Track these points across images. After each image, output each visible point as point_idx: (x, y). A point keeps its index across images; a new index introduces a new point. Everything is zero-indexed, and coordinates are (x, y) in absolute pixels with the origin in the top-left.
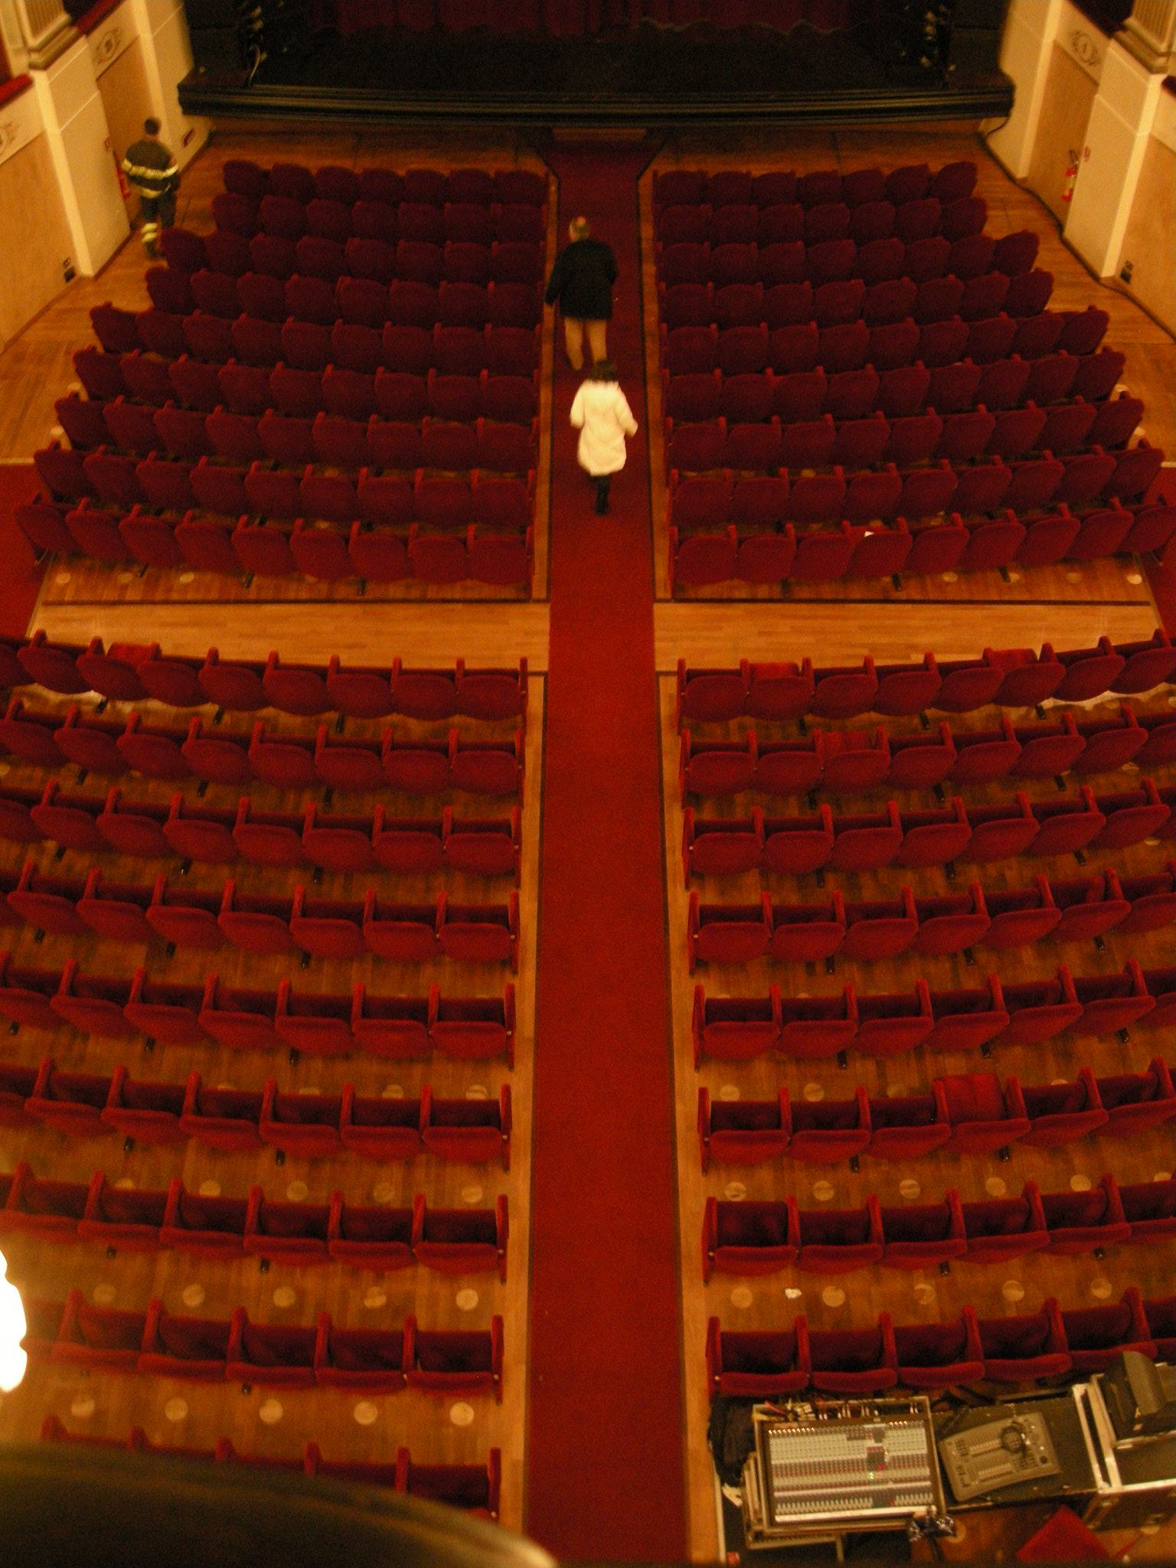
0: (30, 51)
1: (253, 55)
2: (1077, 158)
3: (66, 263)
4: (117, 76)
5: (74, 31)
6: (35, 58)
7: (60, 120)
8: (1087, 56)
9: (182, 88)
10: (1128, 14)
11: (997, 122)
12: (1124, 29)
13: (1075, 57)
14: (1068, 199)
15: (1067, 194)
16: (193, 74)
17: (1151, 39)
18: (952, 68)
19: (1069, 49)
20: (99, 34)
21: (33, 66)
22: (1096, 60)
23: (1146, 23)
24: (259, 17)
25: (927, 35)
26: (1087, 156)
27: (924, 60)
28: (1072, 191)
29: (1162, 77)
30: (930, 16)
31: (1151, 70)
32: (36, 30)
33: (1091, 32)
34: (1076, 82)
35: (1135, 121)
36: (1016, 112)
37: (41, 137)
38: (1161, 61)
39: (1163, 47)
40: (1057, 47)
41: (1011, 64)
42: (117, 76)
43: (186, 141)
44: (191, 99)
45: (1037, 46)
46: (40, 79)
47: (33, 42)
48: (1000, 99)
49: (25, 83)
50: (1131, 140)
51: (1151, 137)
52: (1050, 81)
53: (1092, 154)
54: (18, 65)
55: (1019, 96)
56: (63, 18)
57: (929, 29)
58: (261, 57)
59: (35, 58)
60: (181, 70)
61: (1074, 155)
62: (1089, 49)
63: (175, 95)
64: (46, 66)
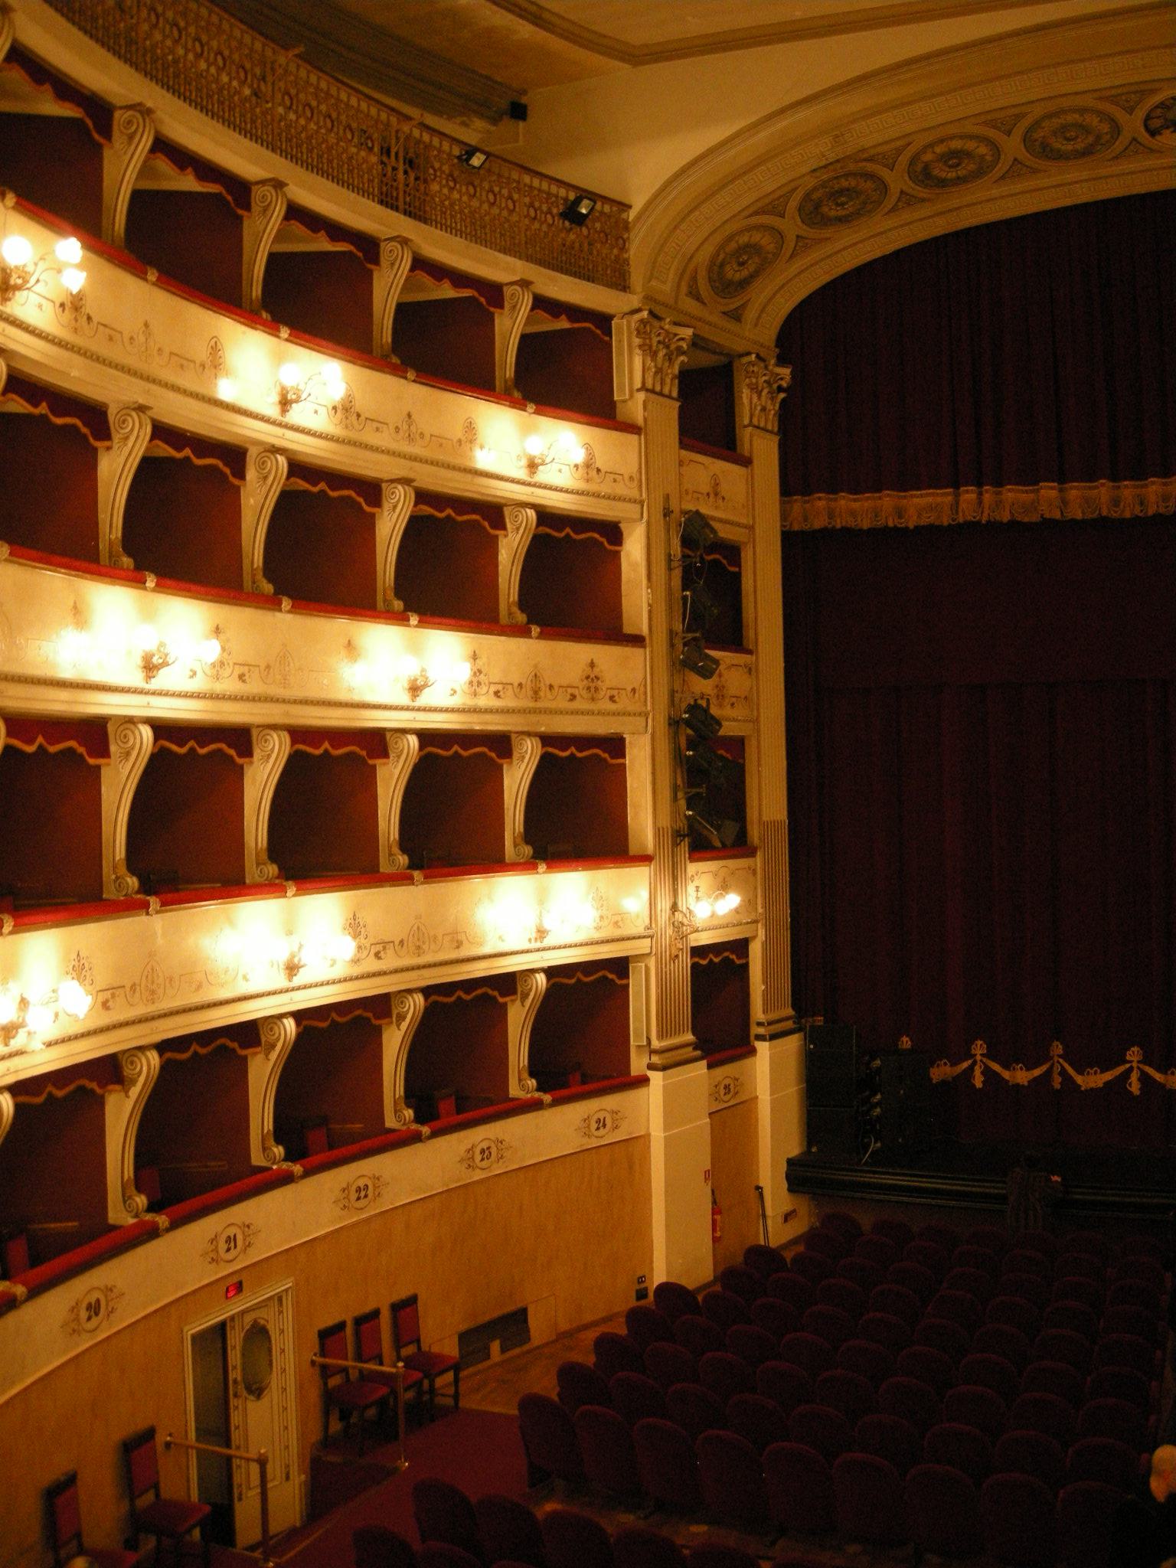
0: (653, 1052)
1: (866, 1147)
3: (641, 1280)
4: (730, 1120)
5: (698, 1053)
6: (655, 1059)
7: (667, 1127)
9: (791, 1162)
16: (808, 1152)
20: (720, 1072)
21: (651, 1067)
24: (878, 1104)
32: (661, 1036)
37: (646, 1137)
42: (730, 1120)
43: (787, 1218)
44: (798, 1176)
46: (656, 1077)
47: (656, 1044)
49: (643, 1081)
54: (638, 1064)
56: (689, 1037)
58: (875, 1145)
59: (655, 1059)
60: (794, 1148)
63: (784, 1167)
64: (664, 1068)
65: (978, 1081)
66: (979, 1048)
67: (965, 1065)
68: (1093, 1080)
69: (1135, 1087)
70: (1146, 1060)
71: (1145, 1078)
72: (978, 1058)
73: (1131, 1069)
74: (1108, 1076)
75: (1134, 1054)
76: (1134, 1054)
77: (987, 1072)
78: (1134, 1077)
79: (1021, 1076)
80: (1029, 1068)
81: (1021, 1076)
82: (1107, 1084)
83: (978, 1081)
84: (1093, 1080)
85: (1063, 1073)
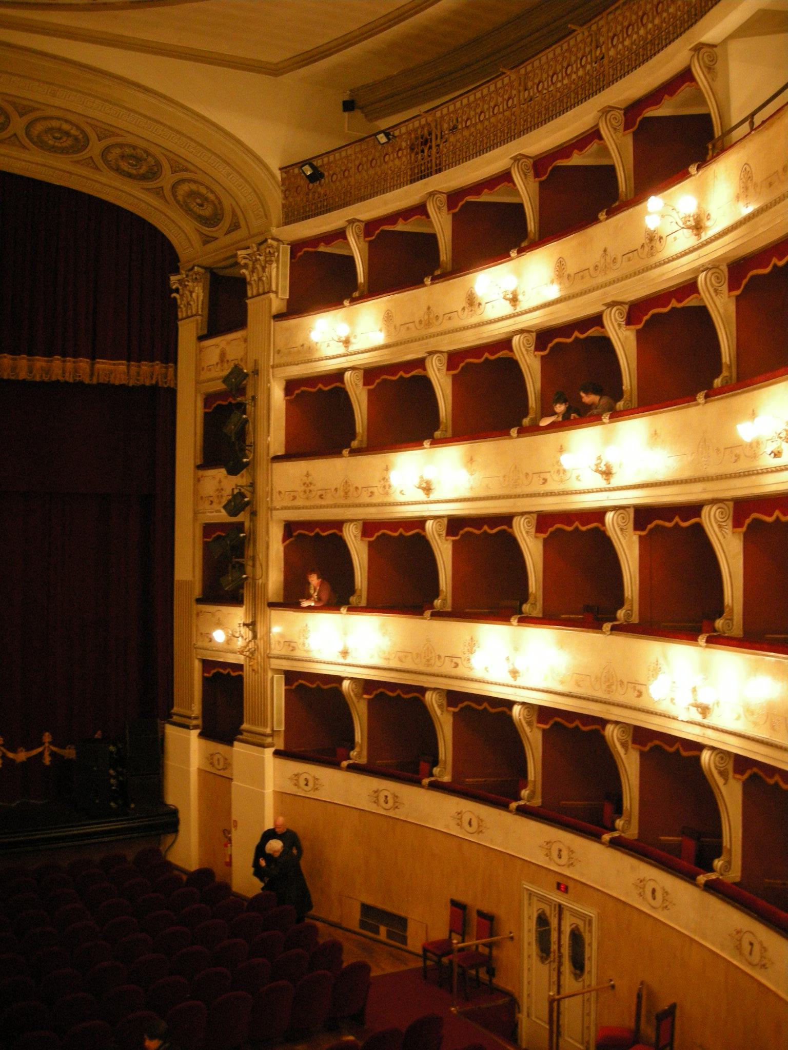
2: (230, 832)
10: (242, 723)
11: (170, 838)
13: (214, 771)
14: (229, 864)
15: (228, 860)
18: (133, 806)
19: (209, 768)
22: (228, 764)
23: (253, 723)
25: (113, 785)
26: (236, 826)
27: (112, 804)
28: (231, 856)
29: (272, 750)
30: (112, 772)
31: (263, 746)
33: (221, 748)
34: (217, 783)
35: (261, 783)
36: (182, 828)
38: (269, 740)
39: (268, 731)
40: (201, 771)
41: (171, 799)
45: (187, 773)
48: (170, 822)
50: (262, 796)
51: (275, 792)
53: (239, 824)
55: (182, 816)
57: (112, 781)
61: (227, 833)
62: (222, 761)
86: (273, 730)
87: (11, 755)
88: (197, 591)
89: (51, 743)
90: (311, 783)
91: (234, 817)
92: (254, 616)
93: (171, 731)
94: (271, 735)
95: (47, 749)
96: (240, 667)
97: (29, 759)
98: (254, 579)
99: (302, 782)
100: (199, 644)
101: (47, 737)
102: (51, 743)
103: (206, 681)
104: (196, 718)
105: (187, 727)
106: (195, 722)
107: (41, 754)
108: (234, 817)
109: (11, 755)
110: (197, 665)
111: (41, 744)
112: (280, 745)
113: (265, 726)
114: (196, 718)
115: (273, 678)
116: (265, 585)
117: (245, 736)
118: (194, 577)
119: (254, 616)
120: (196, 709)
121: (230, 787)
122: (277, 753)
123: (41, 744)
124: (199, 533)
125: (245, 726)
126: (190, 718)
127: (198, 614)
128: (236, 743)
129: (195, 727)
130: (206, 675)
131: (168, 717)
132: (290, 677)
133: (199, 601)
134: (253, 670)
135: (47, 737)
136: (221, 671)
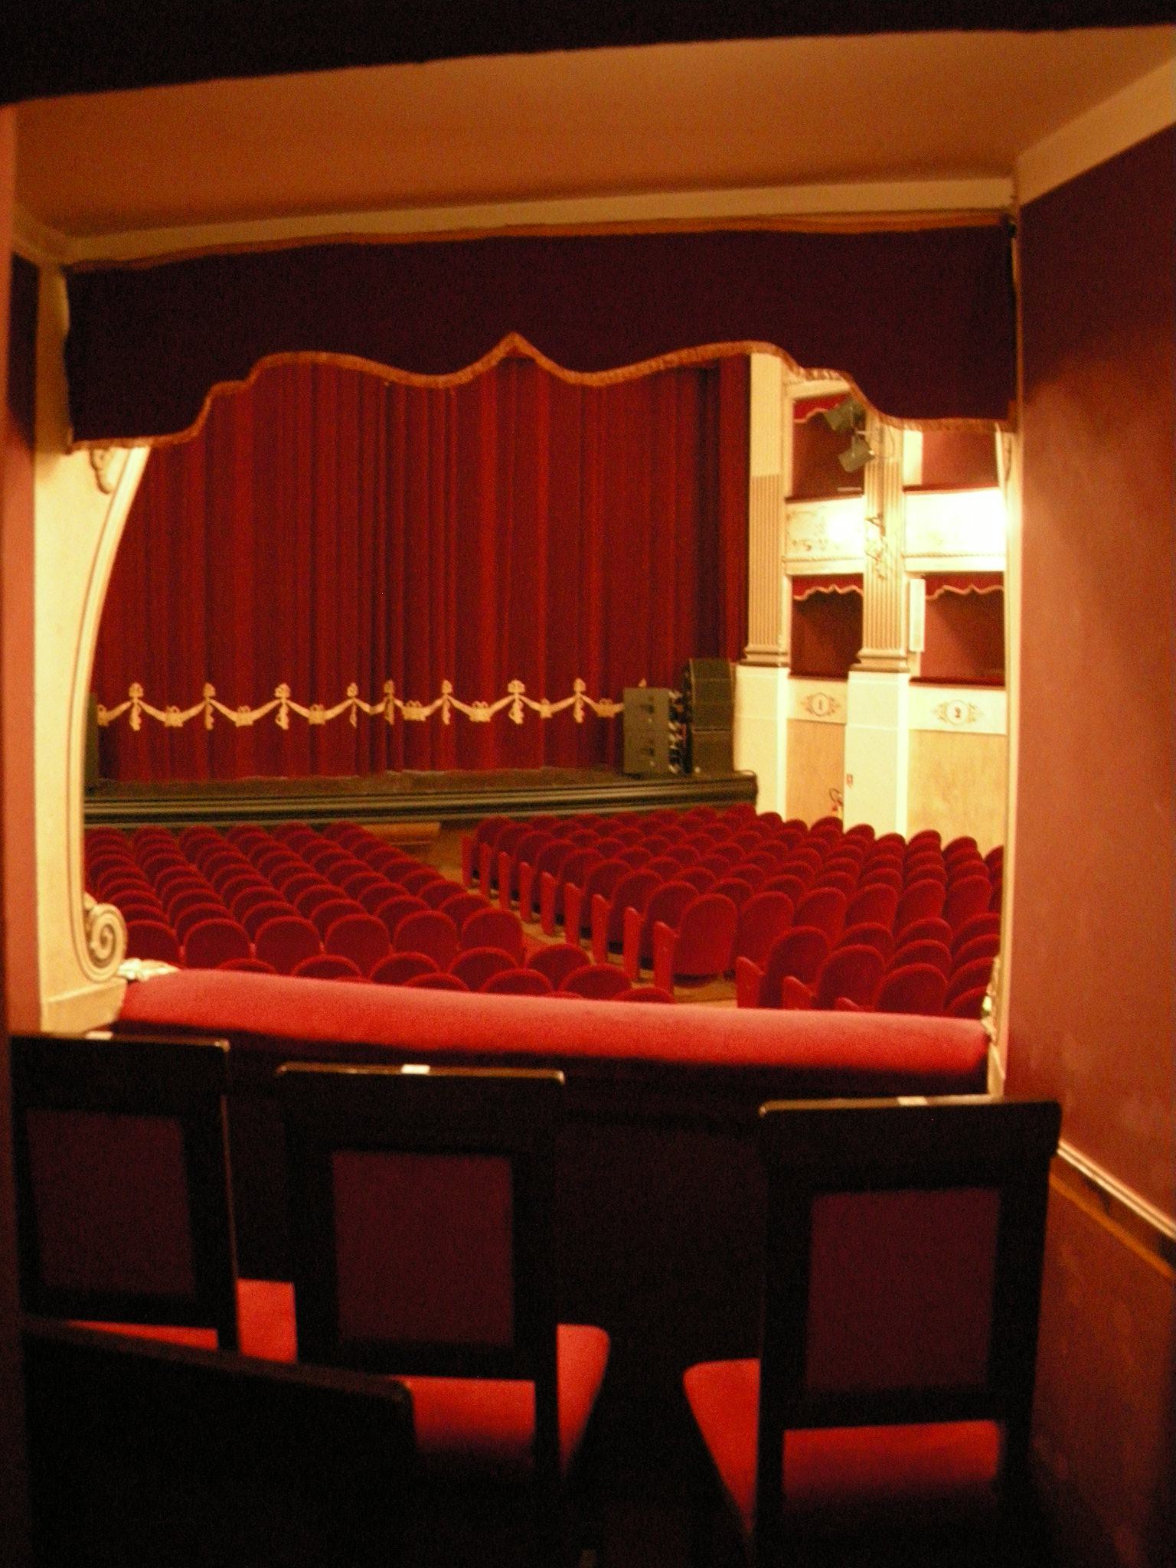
8: (826, 707)
10: (860, 646)
12: (858, 661)
17: (890, 652)
18: (697, 770)
22: (834, 706)
23: (879, 645)
29: (907, 677)
38: (902, 664)
39: (902, 652)
41: (745, 762)
52: (792, 753)
53: (855, 780)
65: (136, 723)
66: (136, 691)
67: (124, 707)
68: (244, 717)
69: (283, 722)
70: (293, 698)
71: (292, 714)
72: (136, 701)
73: (280, 705)
74: (258, 714)
75: (283, 691)
76: (283, 691)
77: (143, 715)
78: (283, 712)
79: (174, 718)
80: (183, 708)
81: (174, 718)
82: (257, 722)
83: (136, 723)
84: (244, 717)
85: (216, 714)
86: (908, 652)
87: (535, 706)
88: (787, 488)
89: (583, 693)
90: (964, 714)
91: (848, 770)
92: (882, 505)
93: (745, 675)
94: (905, 659)
95: (578, 700)
96: (857, 579)
97: (555, 715)
98: (882, 457)
99: (951, 713)
100: (791, 555)
101: (579, 685)
102: (583, 693)
103: (797, 606)
104: (784, 654)
105: (774, 665)
106: (781, 659)
107: (572, 707)
108: (848, 769)
109: (535, 706)
110: (786, 586)
111: (571, 693)
112: (916, 671)
113: (897, 645)
114: (784, 654)
115: (908, 585)
116: (898, 466)
117: (865, 663)
118: (782, 467)
119: (882, 505)
120: (784, 642)
121: (844, 733)
122: (914, 681)
123: (571, 693)
124: (789, 411)
125: (865, 651)
126: (776, 654)
127: (788, 517)
128: (852, 674)
129: (784, 665)
130: (798, 598)
131: (740, 656)
132: (933, 581)
133: (789, 500)
134: (880, 576)
135: (579, 685)
136: (822, 589)
